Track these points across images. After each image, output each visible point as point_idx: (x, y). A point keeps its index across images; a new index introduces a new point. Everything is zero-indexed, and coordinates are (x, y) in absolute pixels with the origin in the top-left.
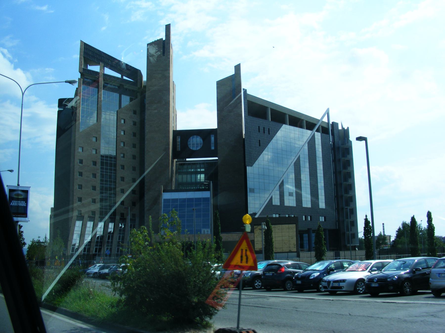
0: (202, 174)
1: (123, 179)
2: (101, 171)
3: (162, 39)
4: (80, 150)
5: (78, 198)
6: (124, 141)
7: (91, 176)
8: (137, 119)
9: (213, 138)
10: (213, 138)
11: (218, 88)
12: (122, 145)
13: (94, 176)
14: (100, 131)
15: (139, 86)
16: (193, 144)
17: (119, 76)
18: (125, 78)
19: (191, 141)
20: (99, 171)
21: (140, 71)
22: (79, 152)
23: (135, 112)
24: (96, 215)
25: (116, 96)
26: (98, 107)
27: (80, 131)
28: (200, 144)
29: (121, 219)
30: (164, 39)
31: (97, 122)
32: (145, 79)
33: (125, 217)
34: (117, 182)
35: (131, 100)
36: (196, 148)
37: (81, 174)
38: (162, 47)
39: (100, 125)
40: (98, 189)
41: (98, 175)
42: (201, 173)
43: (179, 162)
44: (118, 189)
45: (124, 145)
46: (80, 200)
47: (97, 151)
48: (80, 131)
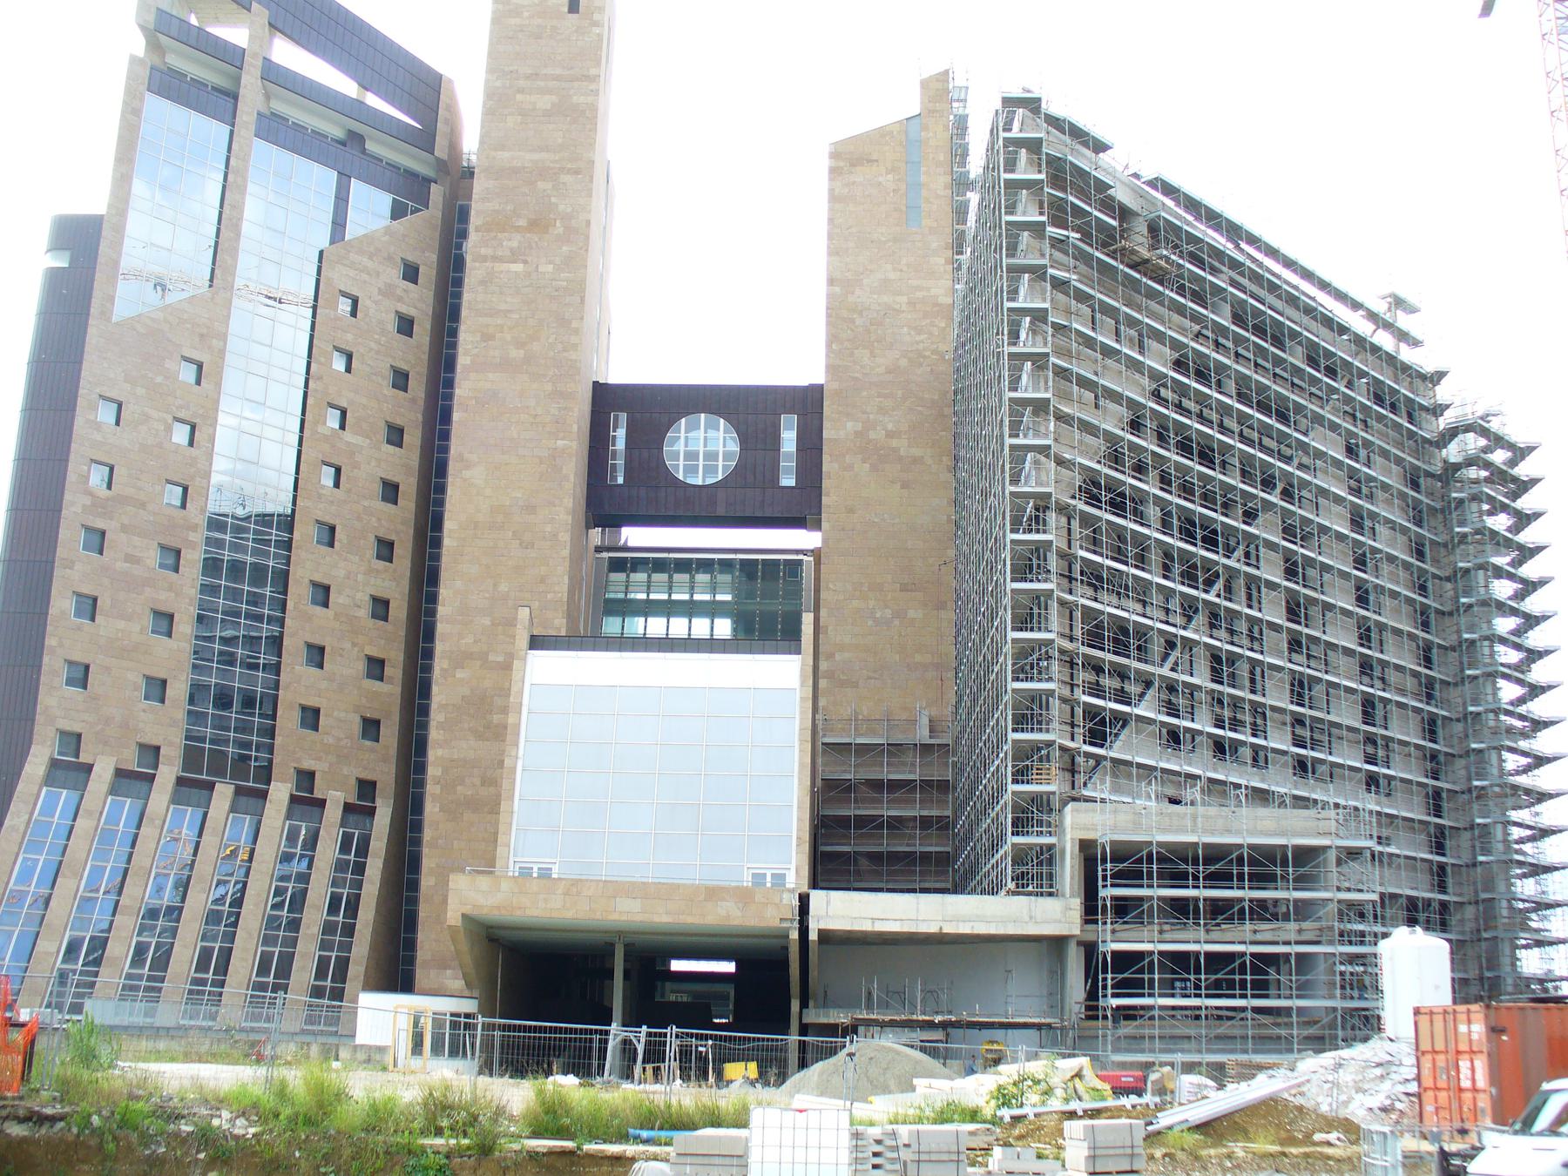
0: (723, 615)
1: (322, 594)
2: (209, 542)
4: (106, 414)
5: (71, 663)
6: (345, 405)
7: (152, 557)
8: (419, 301)
9: (789, 440)
10: (789, 440)
11: (834, 172)
12: (333, 421)
13: (173, 557)
14: (223, 337)
15: (441, 151)
17: (347, 87)
18: (373, 101)
19: (680, 447)
20: (199, 536)
21: (450, 81)
22: (98, 426)
23: (411, 273)
25: (321, 179)
28: (727, 456)
29: (294, 799)
31: (210, 286)
32: (470, 144)
35: (398, 212)
36: (704, 480)
37: (98, 540)
40: (185, 627)
41: (193, 558)
42: (712, 610)
43: (609, 549)
44: (293, 645)
45: (342, 427)
46: (81, 676)
48: (114, 319)
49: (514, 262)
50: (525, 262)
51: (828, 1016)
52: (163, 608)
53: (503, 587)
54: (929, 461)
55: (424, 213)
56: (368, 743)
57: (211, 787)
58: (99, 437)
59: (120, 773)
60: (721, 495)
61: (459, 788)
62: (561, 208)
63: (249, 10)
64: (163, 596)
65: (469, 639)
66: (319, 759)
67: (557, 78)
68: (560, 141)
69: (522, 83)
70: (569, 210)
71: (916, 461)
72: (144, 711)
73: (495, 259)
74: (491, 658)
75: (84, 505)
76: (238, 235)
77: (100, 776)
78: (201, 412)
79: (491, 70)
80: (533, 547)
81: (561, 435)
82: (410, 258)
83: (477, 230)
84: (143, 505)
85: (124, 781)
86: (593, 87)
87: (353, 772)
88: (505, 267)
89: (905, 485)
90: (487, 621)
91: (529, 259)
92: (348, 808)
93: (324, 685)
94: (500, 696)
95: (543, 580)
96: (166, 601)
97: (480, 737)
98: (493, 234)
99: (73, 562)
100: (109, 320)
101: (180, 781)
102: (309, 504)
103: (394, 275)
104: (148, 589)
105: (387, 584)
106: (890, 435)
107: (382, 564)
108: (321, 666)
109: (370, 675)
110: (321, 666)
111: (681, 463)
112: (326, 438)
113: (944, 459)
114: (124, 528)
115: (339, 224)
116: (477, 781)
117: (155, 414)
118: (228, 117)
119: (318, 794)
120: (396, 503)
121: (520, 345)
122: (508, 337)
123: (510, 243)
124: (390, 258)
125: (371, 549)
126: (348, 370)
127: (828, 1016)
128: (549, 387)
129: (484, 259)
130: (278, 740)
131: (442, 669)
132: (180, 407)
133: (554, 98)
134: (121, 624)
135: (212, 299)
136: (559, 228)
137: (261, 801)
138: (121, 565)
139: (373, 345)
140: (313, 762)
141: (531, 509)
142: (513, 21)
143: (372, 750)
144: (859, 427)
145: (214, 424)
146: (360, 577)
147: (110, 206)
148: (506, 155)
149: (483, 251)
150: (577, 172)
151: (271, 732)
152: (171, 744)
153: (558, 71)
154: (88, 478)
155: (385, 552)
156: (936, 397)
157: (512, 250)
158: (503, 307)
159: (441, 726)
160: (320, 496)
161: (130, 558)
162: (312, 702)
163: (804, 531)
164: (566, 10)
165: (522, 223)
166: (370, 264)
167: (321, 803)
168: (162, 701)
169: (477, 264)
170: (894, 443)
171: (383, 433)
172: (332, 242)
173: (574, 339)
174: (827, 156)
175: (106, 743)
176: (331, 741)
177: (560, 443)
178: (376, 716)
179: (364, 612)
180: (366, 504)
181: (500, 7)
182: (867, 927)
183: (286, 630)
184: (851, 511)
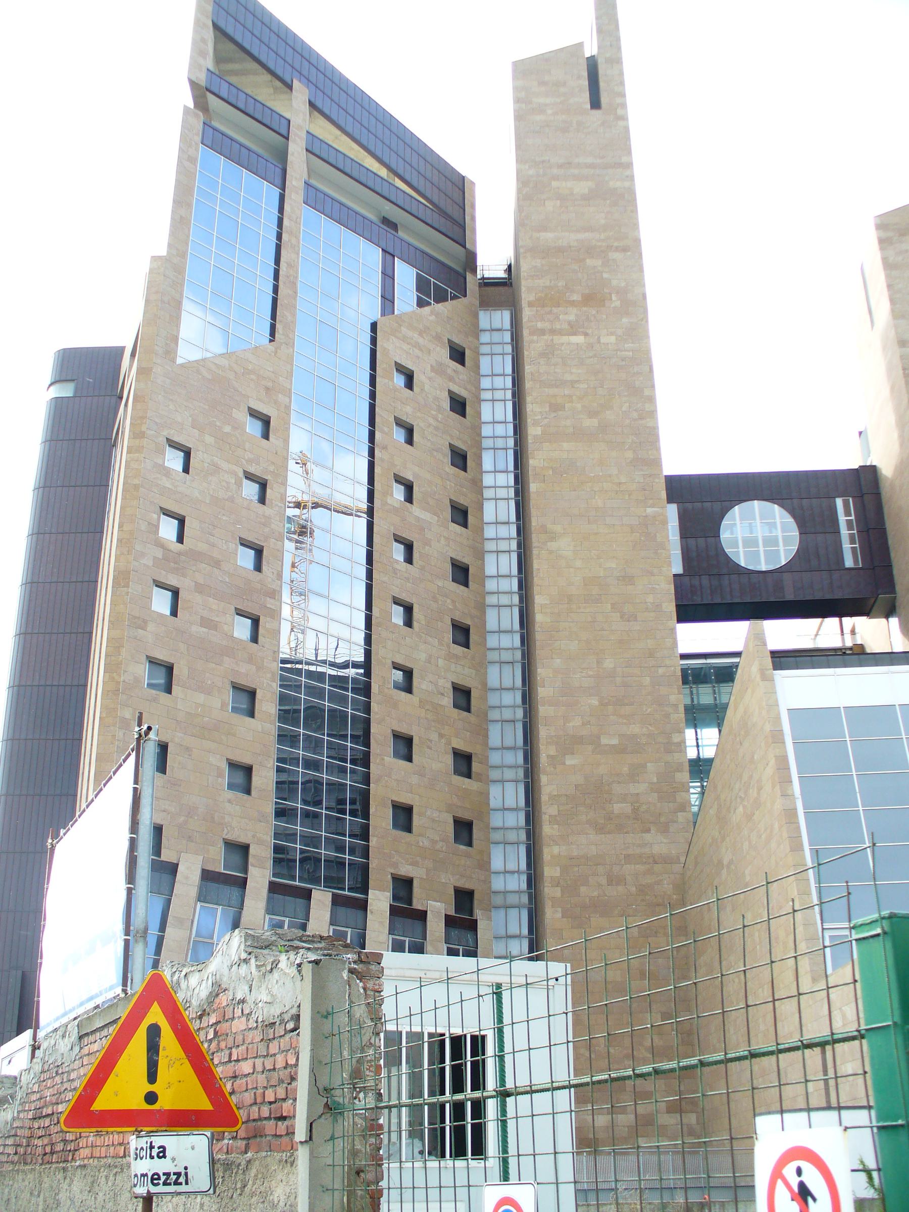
3: (581, 45)
6: (411, 478)
11: (883, 243)
12: (399, 493)
16: (750, 542)
21: (473, 183)
22: (167, 472)
24: (251, 869)
26: (281, 273)
27: (179, 361)
28: (786, 541)
29: (394, 911)
30: (591, 50)
31: (271, 341)
33: (417, 905)
34: (375, 688)
38: (585, 74)
39: (290, 360)
40: (268, 706)
44: (380, 734)
45: (409, 498)
47: (268, 491)
48: (179, 361)
49: (574, 334)
50: (586, 334)
52: (243, 681)
53: (608, 664)
55: (463, 300)
56: (462, 847)
57: (307, 895)
58: (168, 485)
59: (208, 876)
60: (787, 578)
61: (583, 889)
62: (614, 283)
63: (290, 87)
64: (243, 668)
65: (577, 722)
66: (414, 864)
67: (592, 166)
68: (603, 222)
69: (555, 171)
70: (623, 284)
72: (229, 801)
73: (553, 332)
74: (604, 741)
75: (155, 558)
76: (296, 293)
77: (187, 878)
78: (272, 468)
79: (520, 160)
81: (651, 502)
82: (456, 340)
83: (530, 305)
84: (217, 564)
85: (213, 886)
86: (628, 173)
87: (450, 880)
88: (565, 339)
90: (595, 702)
91: (589, 331)
92: (450, 921)
93: (415, 779)
94: (619, 783)
95: (651, 654)
96: (248, 676)
97: (600, 830)
98: (547, 309)
99: (145, 622)
100: (173, 360)
101: (274, 888)
102: (385, 579)
103: (445, 352)
104: (226, 659)
105: (467, 671)
107: (459, 650)
108: (409, 758)
109: (457, 772)
110: (409, 758)
111: (741, 550)
112: (395, 510)
114: (200, 588)
115: (388, 299)
116: (604, 881)
117: (225, 465)
118: (278, 181)
119: (417, 905)
120: (466, 584)
121: (592, 414)
122: (579, 406)
123: (566, 317)
124: (438, 338)
125: (449, 636)
126: (410, 441)
128: (630, 455)
129: (542, 332)
130: (373, 841)
132: (250, 461)
133: (590, 184)
134: (200, 698)
135: (276, 352)
136: (616, 302)
137: (360, 913)
138: (198, 630)
139: (431, 421)
140: (410, 867)
141: (628, 579)
142: (538, 118)
143: (468, 856)
145: (284, 483)
146: (441, 662)
147: (170, 246)
148: (549, 235)
149: (540, 325)
150: (625, 250)
151: (364, 833)
152: (260, 842)
153: (589, 160)
154: (157, 527)
155: (461, 638)
157: (569, 323)
158: (568, 377)
159: (553, 820)
160: (395, 571)
161: (206, 622)
162: (404, 798)
163: (865, 618)
164: (589, 106)
165: (576, 297)
166: (421, 340)
167: (422, 916)
168: (248, 791)
169: (535, 338)
171: (448, 513)
172: (383, 314)
173: (648, 407)
174: (873, 228)
175: (190, 838)
176: (427, 843)
177: (649, 510)
178: (466, 815)
179: (447, 700)
180: (440, 584)
181: (523, 106)
183: (373, 717)
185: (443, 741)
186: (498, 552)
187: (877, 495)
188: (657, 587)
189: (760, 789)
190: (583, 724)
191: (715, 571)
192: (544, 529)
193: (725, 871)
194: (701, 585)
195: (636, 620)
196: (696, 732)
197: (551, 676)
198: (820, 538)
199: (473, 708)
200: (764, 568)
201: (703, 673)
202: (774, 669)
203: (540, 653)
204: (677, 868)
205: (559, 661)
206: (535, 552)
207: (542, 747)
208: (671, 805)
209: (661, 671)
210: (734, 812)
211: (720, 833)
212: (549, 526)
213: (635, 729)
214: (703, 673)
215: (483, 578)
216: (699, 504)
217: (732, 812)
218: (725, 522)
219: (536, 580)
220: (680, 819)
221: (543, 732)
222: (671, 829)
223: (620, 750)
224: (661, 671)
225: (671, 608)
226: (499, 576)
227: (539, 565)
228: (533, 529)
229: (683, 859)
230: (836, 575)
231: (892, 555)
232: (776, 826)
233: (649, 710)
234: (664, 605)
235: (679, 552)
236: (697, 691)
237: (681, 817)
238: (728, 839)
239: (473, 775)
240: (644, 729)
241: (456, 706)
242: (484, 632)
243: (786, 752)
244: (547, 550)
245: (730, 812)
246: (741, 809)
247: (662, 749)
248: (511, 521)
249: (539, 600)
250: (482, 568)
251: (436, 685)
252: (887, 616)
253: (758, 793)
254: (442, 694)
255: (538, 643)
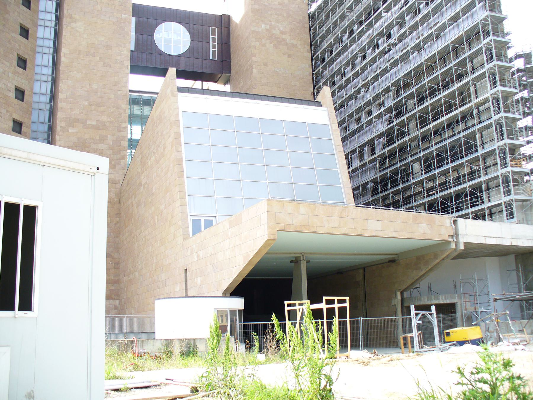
16: (168, 41)
51: (438, 299)
53: (95, 86)
54: (300, 47)
60: (183, 59)
65: (76, 112)
71: (294, 46)
74: (89, 122)
80: (110, 67)
81: (124, 12)
89: (290, 56)
90: (86, 103)
94: (94, 143)
105: (23, 81)
106: (282, 33)
107: (21, 70)
111: (163, 43)
113: (306, 46)
127: (438, 299)
131: (61, 127)
141: (108, 47)
144: (268, 27)
156: (301, 19)
163: (215, 83)
170: (284, 36)
177: (123, 16)
182: (482, 241)
184: (266, 65)
185: (8, 114)
186: (45, 26)
187: (229, 29)
188: (123, 53)
189: (164, 148)
190: (80, 113)
191: (150, 52)
192: (70, 17)
193: (142, 188)
194: (142, 57)
195: (110, 67)
196: (131, 126)
197: (66, 88)
198: (200, 44)
199: (25, 100)
200: (172, 54)
201: (136, 100)
202: (178, 92)
203: (62, 76)
204: (118, 186)
205: (70, 81)
206: (64, 27)
207: (58, 122)
208: (118, 156)
209: (119, 92)
210: (150, 159)
211: (141, 169)
212: (73, 15)
213: (104, 119)
214: (136, 100)
215: (36, 38)
216: (146, 19)
217: (149, 159)
218: (157, 30)
219: (63, 40)
220: (122, 163)
221: (60, 115)
222: (117, 168)
223: (96, 128)
224: (119, 92)
225: (128, 63)
226: (44, 38)
227: (66, 34)
228: (64, 15)
229: (121, 182)
230: (205, 62)
231: (231, 57)
232: (172, 166)
233: (112, 110)
234: (125, 62)
235: (134, 40)
236: (133, 107)
237: (122, 162)
238: (145, 172)
239: (22, 132)
240: (109, 119)
241: (16, 98)
242: (34, 65)
243: (180, 131)
244: (71, 27)
245: (148, 159)
246: (154, 158)
247: (116, 129)
248: (53, 12)
249: (64, 51)
250: (36, 32)
251: (7, 86)
252: (225, 84)
253: (164, 150)
254: (10, 91)
255: (61, 72)
